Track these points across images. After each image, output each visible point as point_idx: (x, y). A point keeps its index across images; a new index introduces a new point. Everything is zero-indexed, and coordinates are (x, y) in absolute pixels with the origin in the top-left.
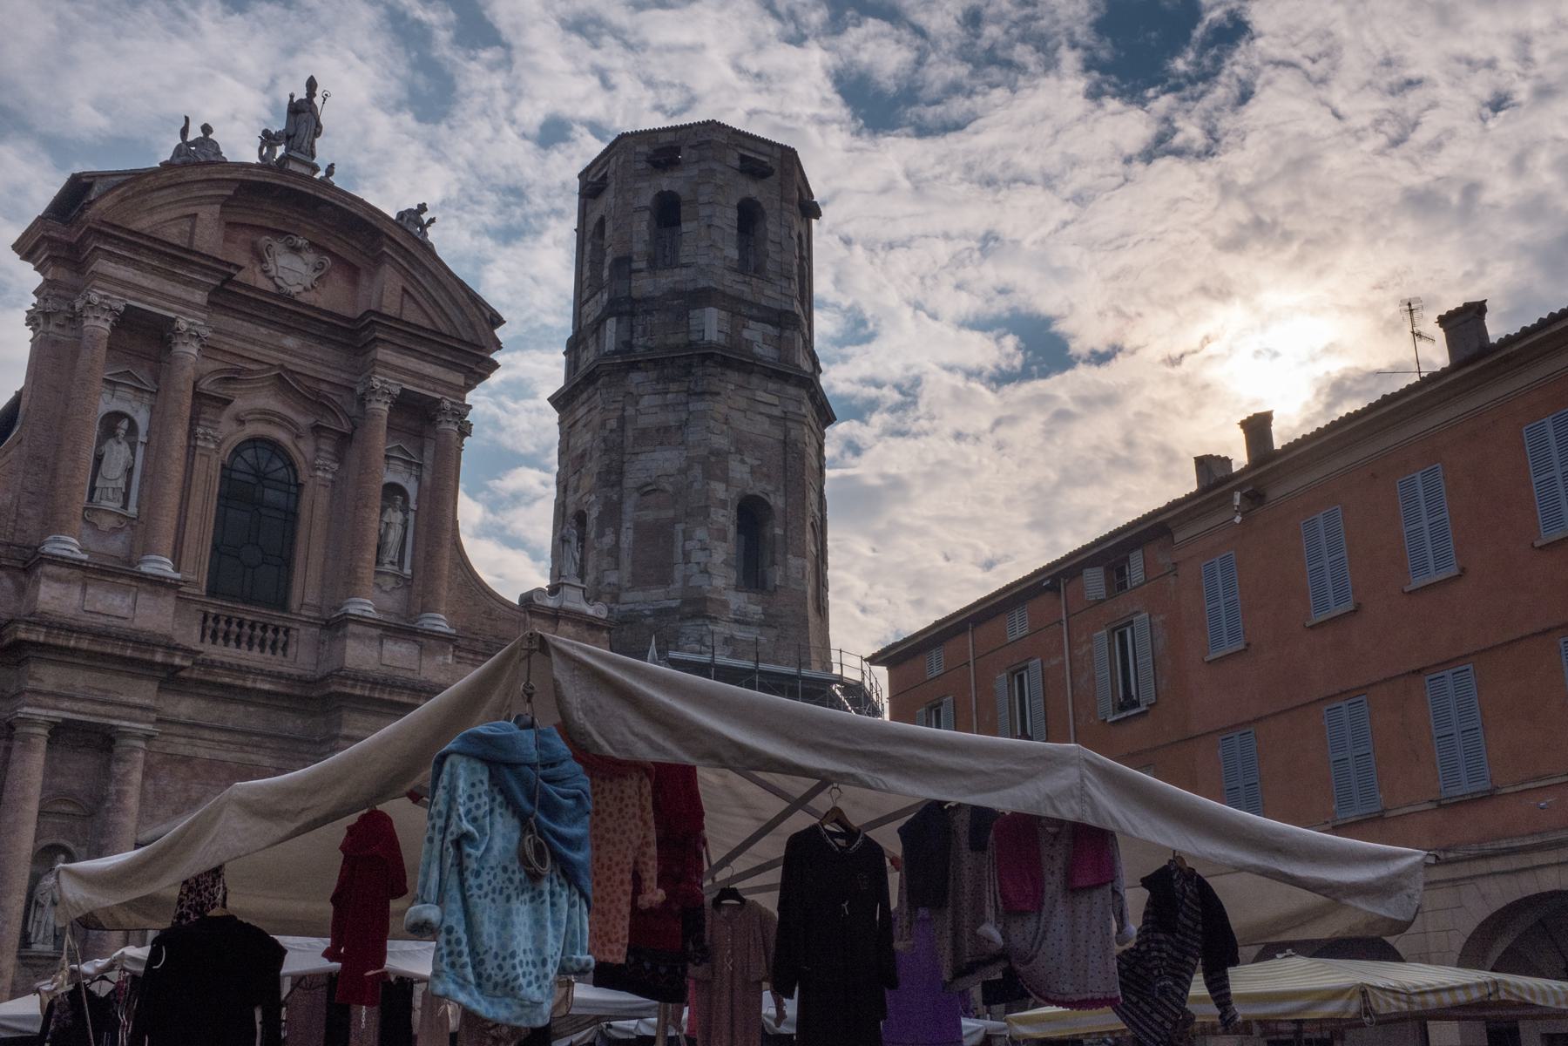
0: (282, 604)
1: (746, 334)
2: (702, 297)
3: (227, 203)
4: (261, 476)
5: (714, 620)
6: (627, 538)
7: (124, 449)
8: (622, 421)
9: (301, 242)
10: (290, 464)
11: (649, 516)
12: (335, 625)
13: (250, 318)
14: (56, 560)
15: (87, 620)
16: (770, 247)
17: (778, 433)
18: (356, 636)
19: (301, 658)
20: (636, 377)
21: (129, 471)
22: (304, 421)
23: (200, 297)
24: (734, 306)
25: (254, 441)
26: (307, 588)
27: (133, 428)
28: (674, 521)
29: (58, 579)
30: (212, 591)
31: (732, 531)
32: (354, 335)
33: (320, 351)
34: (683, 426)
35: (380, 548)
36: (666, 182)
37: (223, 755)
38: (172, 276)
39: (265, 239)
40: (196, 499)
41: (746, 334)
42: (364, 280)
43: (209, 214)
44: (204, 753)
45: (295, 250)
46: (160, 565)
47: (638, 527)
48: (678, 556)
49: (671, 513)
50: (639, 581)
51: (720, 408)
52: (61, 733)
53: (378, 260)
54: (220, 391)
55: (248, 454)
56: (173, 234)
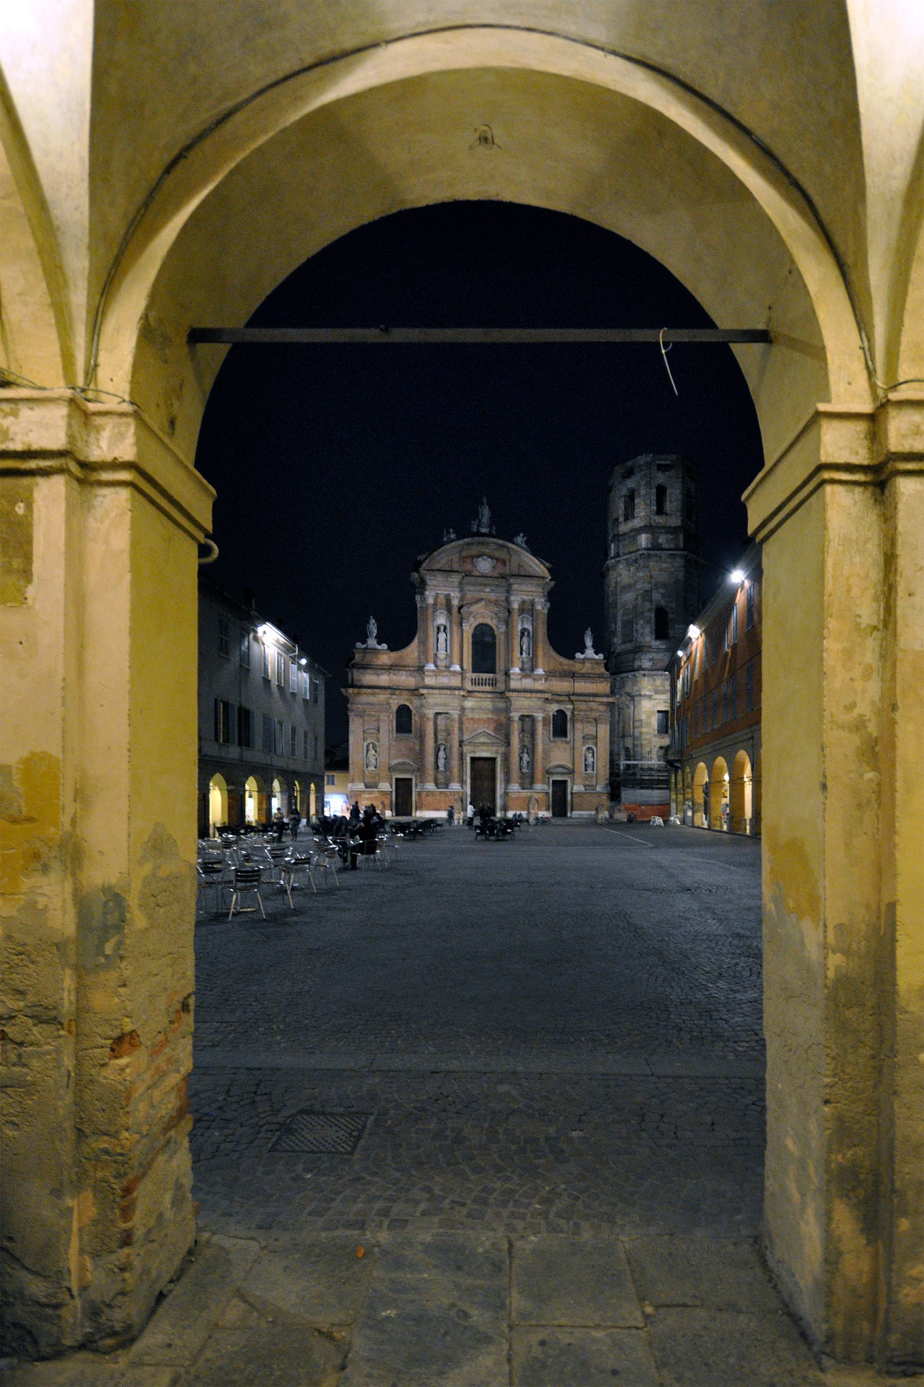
1: (660, 541)
10: (491, 628)
14: (429, 671)
15: (438, 686)
23: (456, 584)
25: (481, 625)
26: (500, 664)
27: (445, 628)
31: (653, 621)
35: (522, 649)
44: (476, 716)
47: (623, 622)
56: (447, 568)
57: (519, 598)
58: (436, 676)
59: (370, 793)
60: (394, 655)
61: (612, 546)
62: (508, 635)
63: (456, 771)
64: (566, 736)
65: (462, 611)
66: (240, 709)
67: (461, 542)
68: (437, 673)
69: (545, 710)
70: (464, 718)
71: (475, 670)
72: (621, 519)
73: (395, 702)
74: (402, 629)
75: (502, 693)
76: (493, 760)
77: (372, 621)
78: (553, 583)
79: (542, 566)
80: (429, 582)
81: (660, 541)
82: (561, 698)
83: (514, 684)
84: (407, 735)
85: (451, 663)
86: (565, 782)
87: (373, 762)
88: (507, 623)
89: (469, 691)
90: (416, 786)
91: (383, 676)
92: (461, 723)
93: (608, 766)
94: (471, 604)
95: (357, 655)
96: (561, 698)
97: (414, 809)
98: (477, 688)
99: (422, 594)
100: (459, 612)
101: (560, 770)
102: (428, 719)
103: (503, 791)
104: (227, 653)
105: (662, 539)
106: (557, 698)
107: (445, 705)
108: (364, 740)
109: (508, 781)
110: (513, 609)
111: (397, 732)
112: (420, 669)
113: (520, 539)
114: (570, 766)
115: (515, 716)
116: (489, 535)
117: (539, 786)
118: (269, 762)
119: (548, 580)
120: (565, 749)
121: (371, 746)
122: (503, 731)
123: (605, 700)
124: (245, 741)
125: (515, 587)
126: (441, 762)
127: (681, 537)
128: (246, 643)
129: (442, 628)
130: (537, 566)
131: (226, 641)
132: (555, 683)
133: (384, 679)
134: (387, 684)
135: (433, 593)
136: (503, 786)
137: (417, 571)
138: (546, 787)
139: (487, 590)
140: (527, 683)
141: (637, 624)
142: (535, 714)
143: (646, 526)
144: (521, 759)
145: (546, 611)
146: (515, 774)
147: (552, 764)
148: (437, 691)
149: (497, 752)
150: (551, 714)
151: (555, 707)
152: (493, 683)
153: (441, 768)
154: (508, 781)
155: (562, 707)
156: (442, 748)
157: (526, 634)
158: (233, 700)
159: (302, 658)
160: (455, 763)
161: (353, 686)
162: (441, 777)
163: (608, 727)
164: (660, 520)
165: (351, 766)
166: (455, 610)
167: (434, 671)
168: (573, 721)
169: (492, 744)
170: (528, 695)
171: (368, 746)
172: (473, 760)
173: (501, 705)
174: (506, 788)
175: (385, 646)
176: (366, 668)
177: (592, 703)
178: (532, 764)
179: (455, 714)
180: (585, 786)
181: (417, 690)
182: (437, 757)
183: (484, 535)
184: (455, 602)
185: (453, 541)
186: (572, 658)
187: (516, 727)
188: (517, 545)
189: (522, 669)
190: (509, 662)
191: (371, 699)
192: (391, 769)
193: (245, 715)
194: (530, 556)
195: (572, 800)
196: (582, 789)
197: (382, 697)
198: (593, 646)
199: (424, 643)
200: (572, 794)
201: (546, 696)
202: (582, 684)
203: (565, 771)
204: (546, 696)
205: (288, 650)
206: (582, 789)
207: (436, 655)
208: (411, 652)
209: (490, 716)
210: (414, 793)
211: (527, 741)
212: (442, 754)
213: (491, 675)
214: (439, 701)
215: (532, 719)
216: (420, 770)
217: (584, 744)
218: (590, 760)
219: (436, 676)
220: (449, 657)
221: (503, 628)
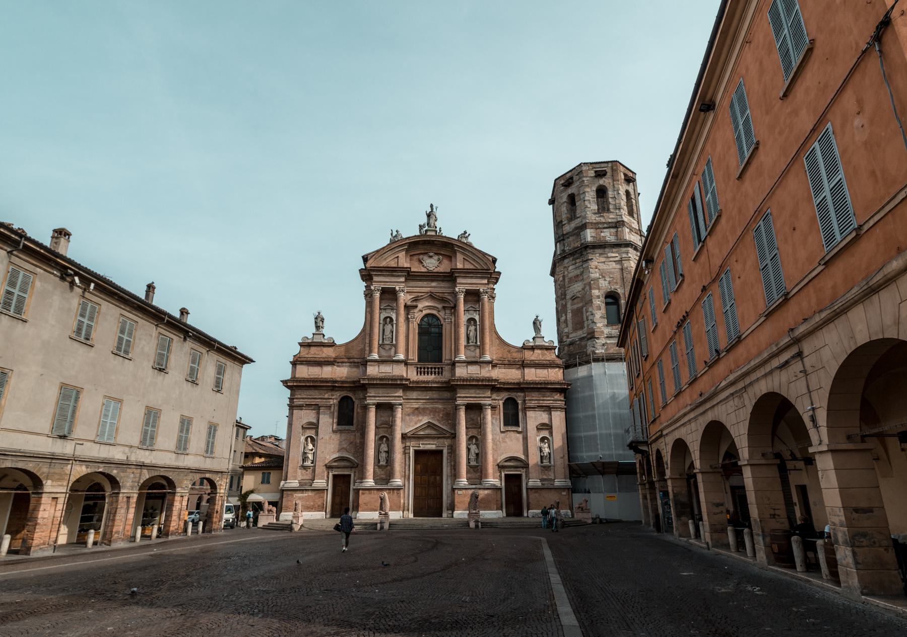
0: (441, 361)
2: (584, 227)
3: (407, 251)
4: (430, 325)
5: (598, 338)
6: (569, 315)
7: (390, 326)
8: (564, 277)
9: (431, 254)
10: (438, 319)
11: (575, 307)
12: (453, 364)
13: (420, 280)
16: (610, 200)
17: (619, 266)
19: (446, 376)
20: (566, 261)
22: (440, 306)
23: (403, 279)
24: (596, 226)
25: (427, 315)
26: (446, 356)
28: (582, 307)
30: (419, 360)
32: (450, 277)
33: (442, 284)
34: (582, 273)
36: (570, 191)
38: (393, 276)
39: (421, 257)
40: (411, 336)
41: (602, 234)
42: (453, 259)
43: (402, 255)
45: (431, 257)
46: (401, 356)
48: (585, 319)
49: (580, 305)
50: (575, 329)
51: (593, 264)
52: (379, 406)
53: (455, 252)
54: (414, 304)
55: (426, 319)
56: (393, 264)
64: (517, 425)
84: (347, 427)
86: (520, 476)
87: (310, 456)
90: (355, 482)
103: (450, 487)
109: (455, 475)
114: (523, 457)
120: (518, 439)
141: (587, 312)
163: (563, 414)
171: (307, 438)
178: (480, 457)
180: (542, 480)
200: (527, 489)
206: (539, 484)
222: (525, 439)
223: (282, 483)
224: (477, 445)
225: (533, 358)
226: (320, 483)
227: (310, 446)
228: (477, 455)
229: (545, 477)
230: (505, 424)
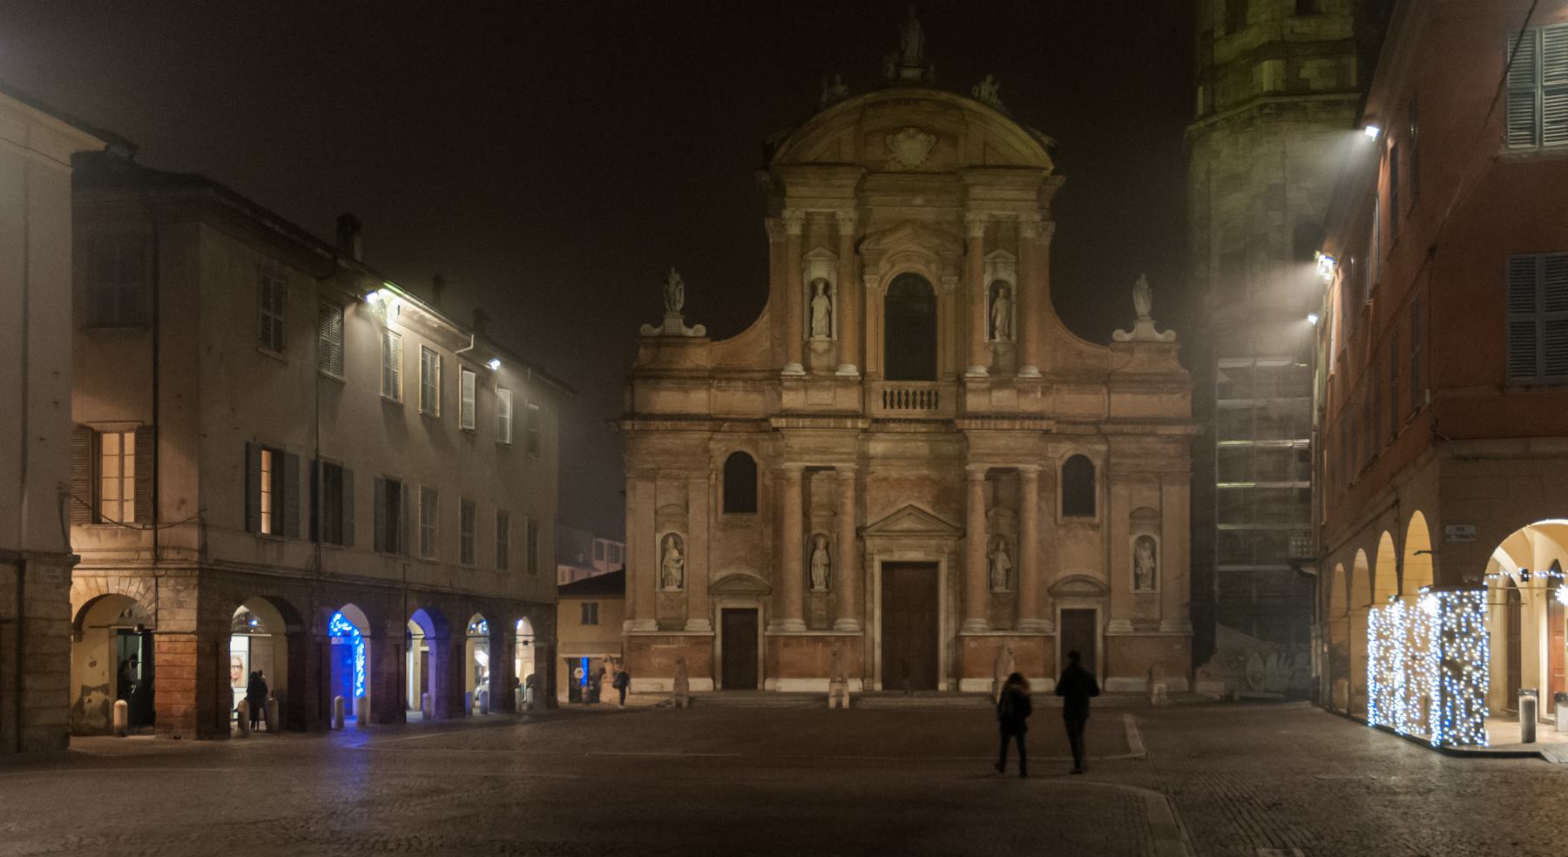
1: (1304, 74)
10: (927, 283)
18: (972, 391)
21: (829, 313)
23: (849, 192)
25: (903, 278)
26: (945, 360)
27: (827, 287)
29: (790, 389)
37: (907, 473)
44: (895, 474)
45: (913, 137)
46: (850, 370)
57: (984, 217)
58: (806, 390)
59: (667, 640)
60: (720, 347)
61: (1201, 89)
62: (964, 299)
63: (848, 592)
64: (1091, 512)
65: (862, 248)
66: (314, 466)
67: (860, 101)
68: (812, 379)
69: (1042, 457)
70: (869, 479)
71: (889, 376)
72: (1220, 32)
73: (722, 448)
74: (735, 292)
75: (948, 422)
76: (933, 566)
77: (675, 277)
78: (1060, 180)
79: (1034, 144)
80: (791, 191)
81: (1304, 74)
82: (1080, 429)
83: (974, 402)
84: (745, 517)
85: (839, 361)
86: (1090, 614)
87: (676, 574)
88: (961, 270)
89: (877, 421)
90: (766, 624)
91: (698, 394)
92: (861, 488)
93: (1188, 576)
94: (884, 233)
95: (642, 351)
96: (1080, 429)
97: (761, 674)
98: (894, 413)
99: (778, 215)
100: (857, 251)
101: (1079, 587)
102: (788, 480)
103: (952, 634)
104: (280, 348)
105: (1310, 70)
106: (1070, 429)
107: (825, 451)
108: (656, 530)
109: (962, 613)
110: (973, 239)
111: (726, 511)
112: (774, 378)
113: (987, 88)
114: (1101, 577)
115: (978, 470)
116: (922, 83)
117: (1029, 622)
118: (399, 576)
119: (1047, 173)
121: (671, 540)
122: (951, 500)
123: (1177, 430)
124: (330, 526)
125: (977, 192)
126: (819, 574)
127: (1352, 62)
128: (335, 326)
129: (821, 287)
130: (1024, 145)
131: (279, 323)
132: (1067, 397)
133: (698, 400)
134: (704, 410)
135: (800, 214)
136: (952, 624)
137: (766, 168)
138: (1046, 625)
139: (919, 201)
140: (1004, 399)
142: (1021, 466)
143: (1272, 43)
144: (992, 563)
145: (1046, 242)
146: (978, 595)
147: (1062, 574)
148: (807, 422)
149: (940, 551)
150: (1059, 464)
151: (1067, 450)
152: (931, 400)
153: (819, 587)
154: (962, 613)
155: (1084, 449)
156: (821, 542)
157: (1001, 291)
158: (296, 442)
159: (490, 358)
160: (847, 574)
161: (632, 415)
162: (819, 607)
164: (1305, 27)
165: (629, 585)
166: (846, 247)
167: (799, 379)
168: (1108, 481)
169: (929, 534)
170: (1006, 424)
171: (665, 541)
172: (887, 567)
173: (948, 448)
174: (958, 631)
175: (700, 330)
176: (661, 378)
177: (1150, 439)
178: (1015, 574)
179: (847, 469)
180: (1134, 621)
181: (765, 420)
182: (808, 563)
183: (912, 84)
184: (847, 230)
185: (841, 100)
186: (1104, 339)
187: (979, 496)
188: (978, 99)
189: (992, 371)
190: (965, 357)
191: (670, 442)
192: (714, 590)
193: (332, 480)
194: (1008, 123)
195: (1106, 650)
196: (1128, 627)
197: (694, 437)
198: (1154, 314)
199: (781, 319)
200: (1105, 638)
201: (1045, 425)
202: (1128, 397)
203: (1091, 589)
204: (1045, 425)
205: (451, 342)
207: (806, 347)
208: (756, 340)
209: (926, 472)
210: (760, 640)
211: (1005, 525)
212: (820, 556)
213: (926, 384)
214: (811, 442)
215: (1016, 476)
216: (774, 592)
217: (1132, 528)
218: (1146, 564)
219: (806, 390)
220: (836, 347)
221: (951, 282)
222: (1108, 540)
223: (626, 625)
224: (1007, 551)
225: (1129, 369)
226: (699, 626)
227: (675, 554)
228: (1008, 571)
229: (1141, 615)
230: (1066, 512)
